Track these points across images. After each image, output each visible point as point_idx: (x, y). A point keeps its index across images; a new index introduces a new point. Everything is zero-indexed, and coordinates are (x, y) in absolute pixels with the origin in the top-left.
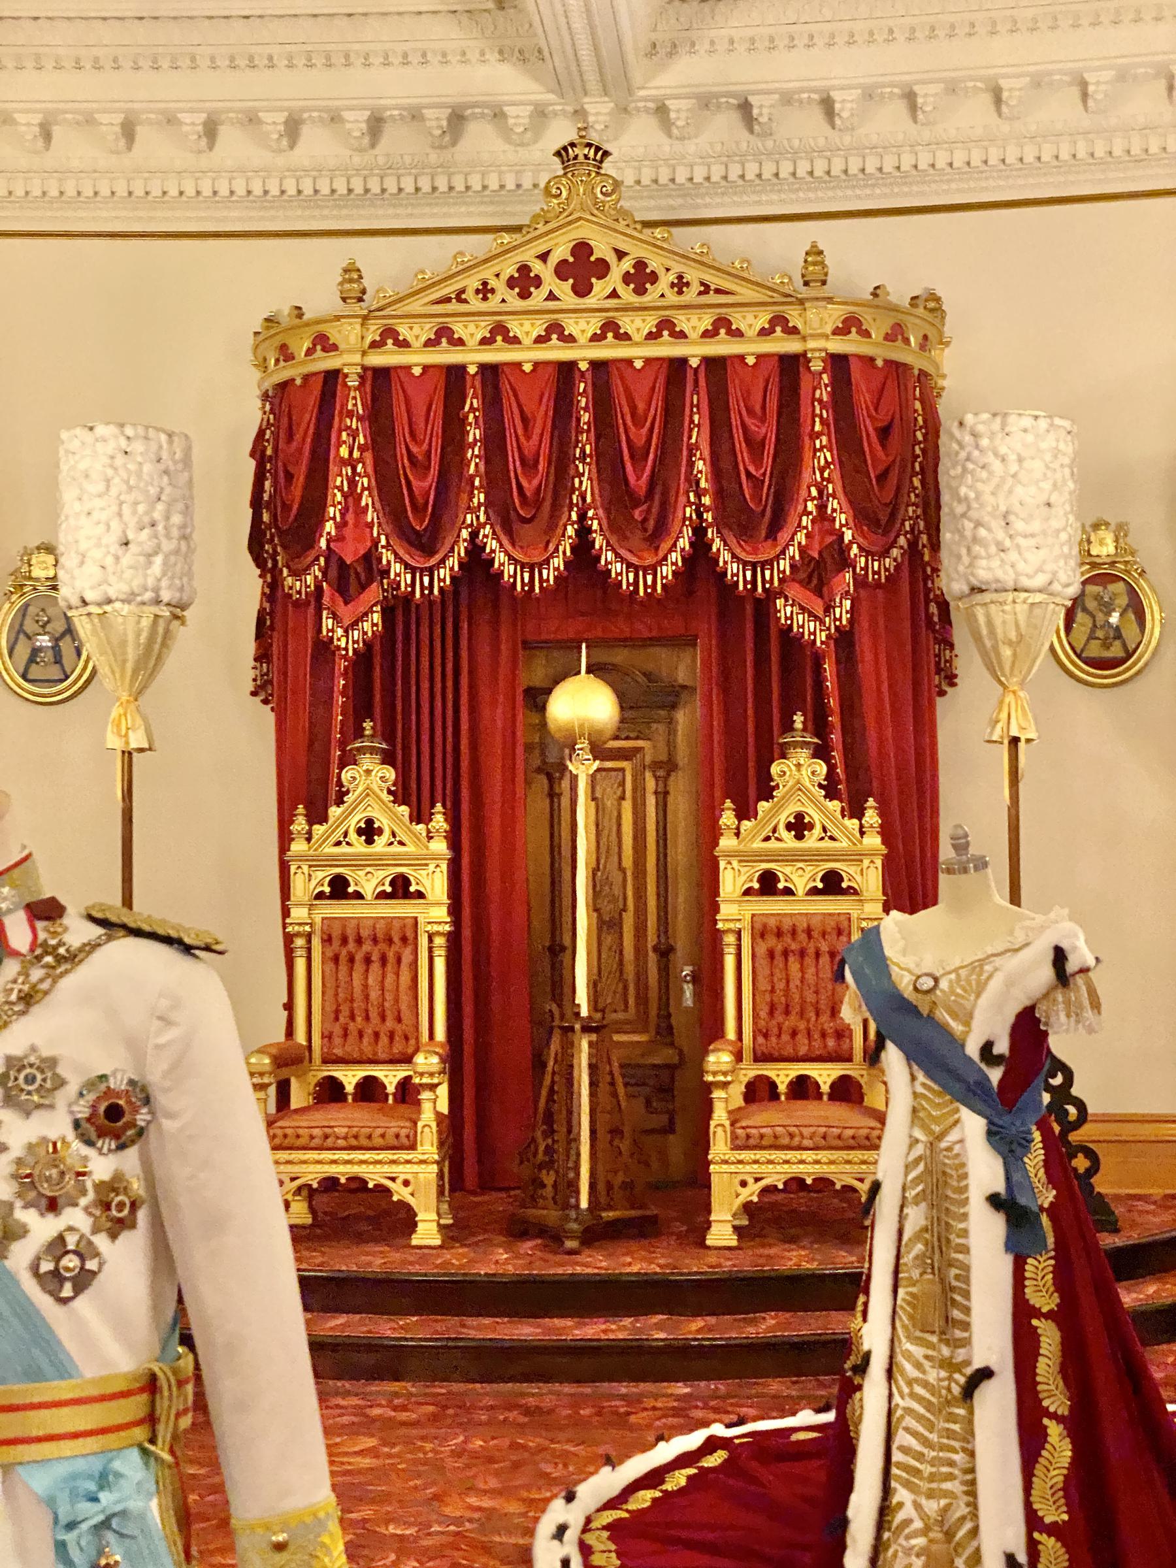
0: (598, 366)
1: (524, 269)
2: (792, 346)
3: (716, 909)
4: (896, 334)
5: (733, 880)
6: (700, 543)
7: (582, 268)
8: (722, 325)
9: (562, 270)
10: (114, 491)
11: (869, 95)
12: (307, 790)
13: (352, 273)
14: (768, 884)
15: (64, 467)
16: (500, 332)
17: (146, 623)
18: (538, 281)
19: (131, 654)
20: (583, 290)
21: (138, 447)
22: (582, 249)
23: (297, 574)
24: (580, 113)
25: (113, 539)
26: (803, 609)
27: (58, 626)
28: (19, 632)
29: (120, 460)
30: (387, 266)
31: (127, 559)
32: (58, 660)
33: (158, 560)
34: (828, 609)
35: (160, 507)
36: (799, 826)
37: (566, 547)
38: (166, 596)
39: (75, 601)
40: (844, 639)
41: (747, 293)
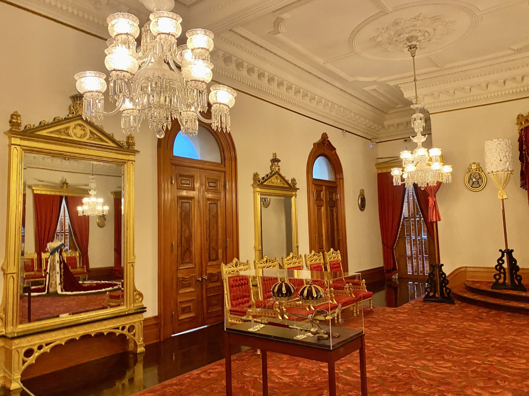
10: (498, 151)
15: (486, 148)
17: (506, 175)
19: (503, 181)
21: (502, 142)
25: (499, 159)
27: (478, 177)
28: (470, 178)
29: (498, 145)
31: (502, 163)
32: (478, 183)
33: (508, 163)
35: (507, 153)
38: (510, 169)
39: (490, 172)
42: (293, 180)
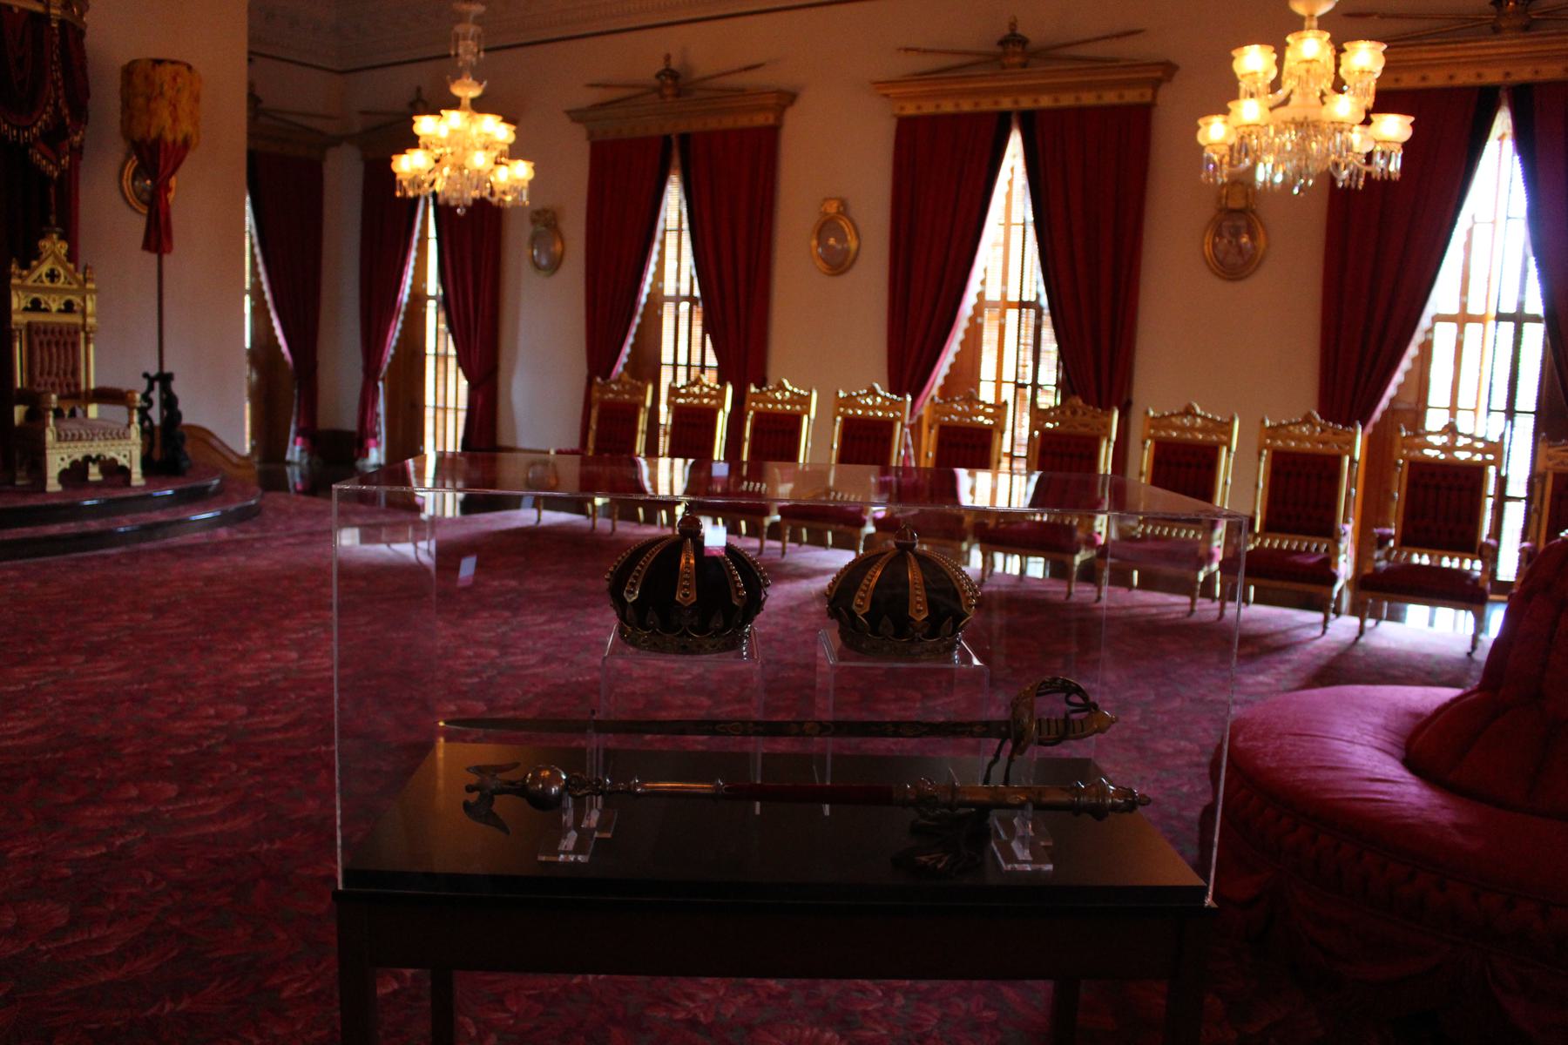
3: (10, 317)
5: (17, 301)
14: (36, 306)
26: (44, 157)
34: (59, 160)
36: (52, 276)
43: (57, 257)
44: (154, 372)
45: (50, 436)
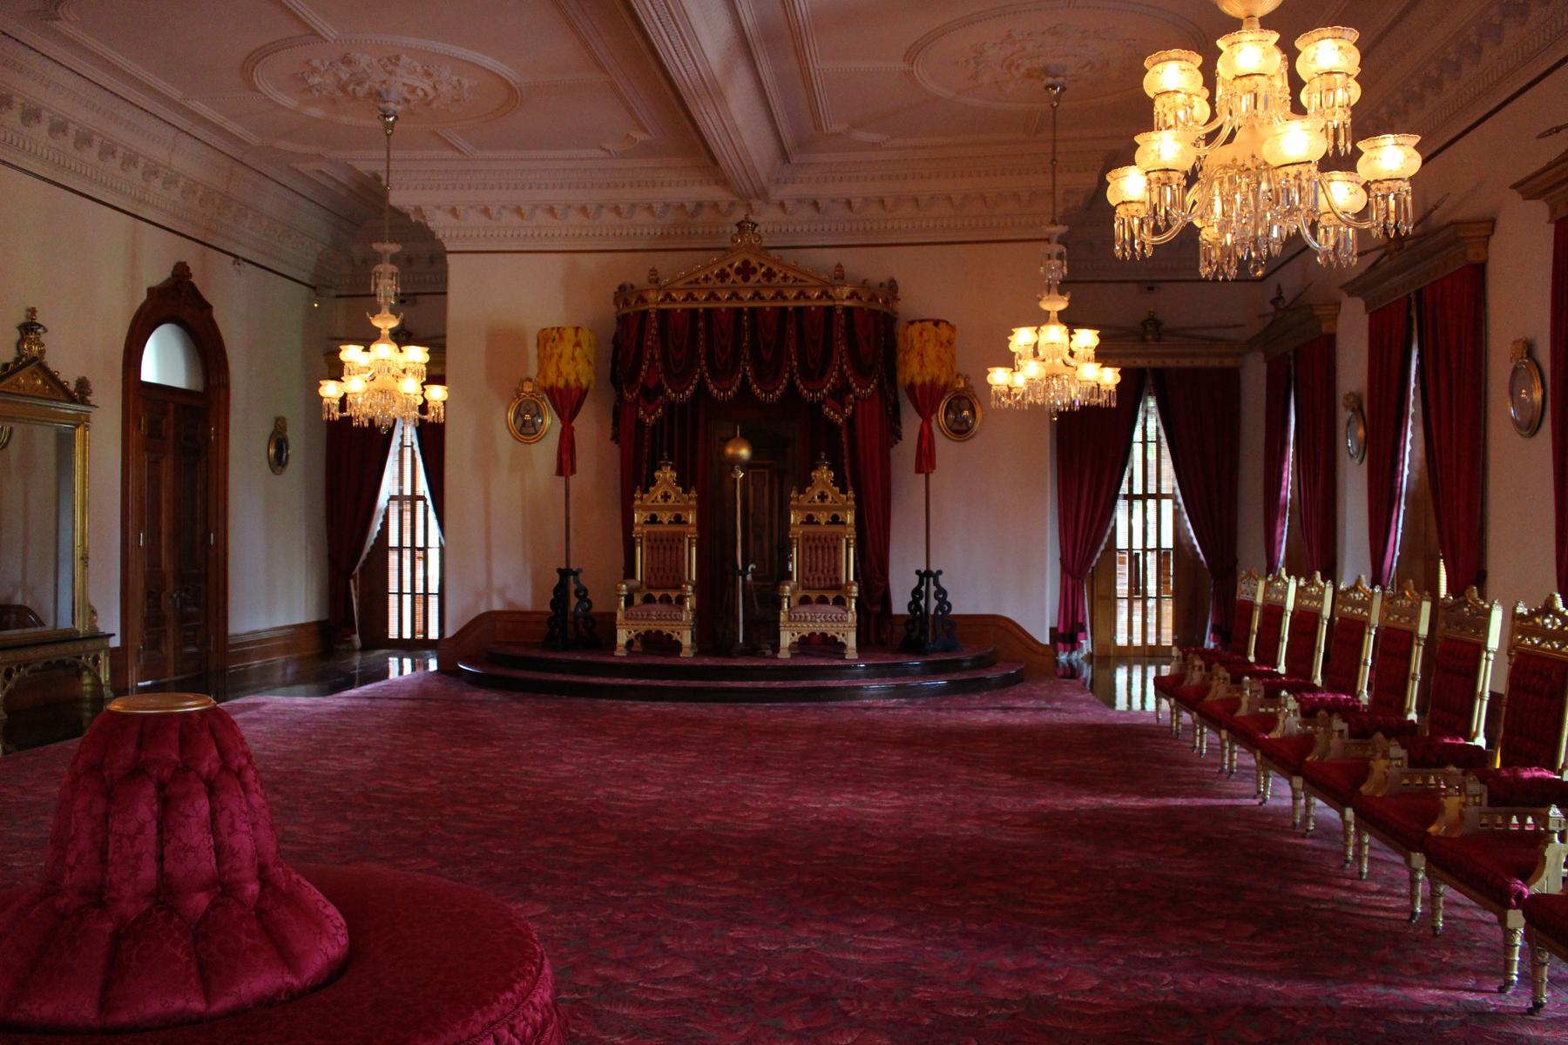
0: (751, 309)
1: (723, 270)
2: (830, 303)
4: (874, 298)
6: (791, 382)
7: (746, 271)
8: (802, 294)
9: (738, 271)
11: (866, 200)
12: (635, 478)
13: (654, 271)
14: (810, 520)
16: (712, 296)
18: (728, 276)
20: (746, 279)
22: (746, 263)
23: (630, 392)
24: (749, 205)
30: (667, 265)
37: (738, 382)
40: (850, 421)
41: (812, 282)
42: (83, 384)
43: (824, 483)
44: (923, 569)
45: (783, 617)
